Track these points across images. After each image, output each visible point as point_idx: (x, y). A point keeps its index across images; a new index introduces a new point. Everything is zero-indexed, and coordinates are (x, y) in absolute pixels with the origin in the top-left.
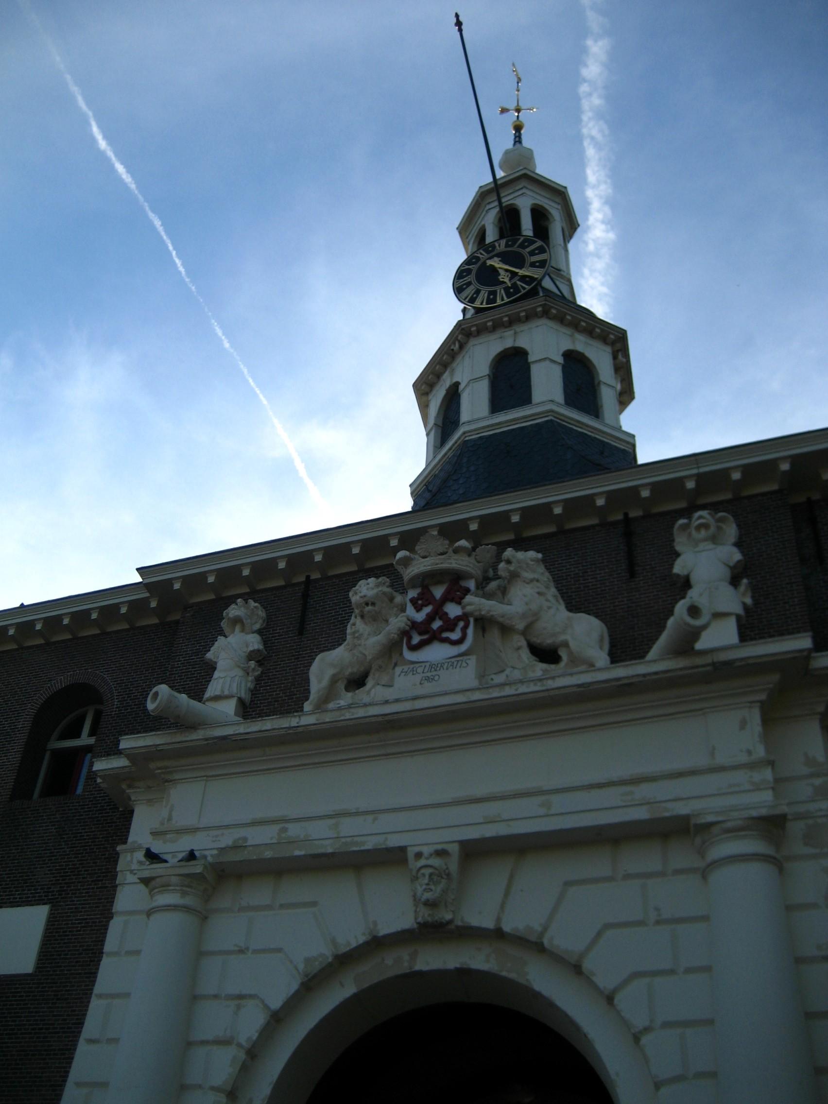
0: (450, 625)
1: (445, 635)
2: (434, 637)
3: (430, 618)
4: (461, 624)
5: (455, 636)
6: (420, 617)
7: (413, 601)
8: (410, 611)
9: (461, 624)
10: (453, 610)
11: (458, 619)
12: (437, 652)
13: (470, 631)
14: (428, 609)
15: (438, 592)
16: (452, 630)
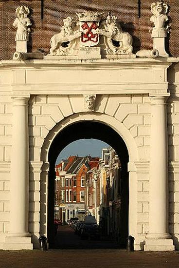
0: (93, 36)
1: (92, 39)
2: (90, 39)
3: (88, 33)
4: (96, 36)
5: (95, 39)
6: (85, 32)
7: (83, 26)
8: (81, 29)
9: (96, 36)
10: (94, 31)
11: (95, 35)
12: (90, 44)
13: (98, 39)
14: (87, 30)
15: (90, 25)
16: (94, 38)
